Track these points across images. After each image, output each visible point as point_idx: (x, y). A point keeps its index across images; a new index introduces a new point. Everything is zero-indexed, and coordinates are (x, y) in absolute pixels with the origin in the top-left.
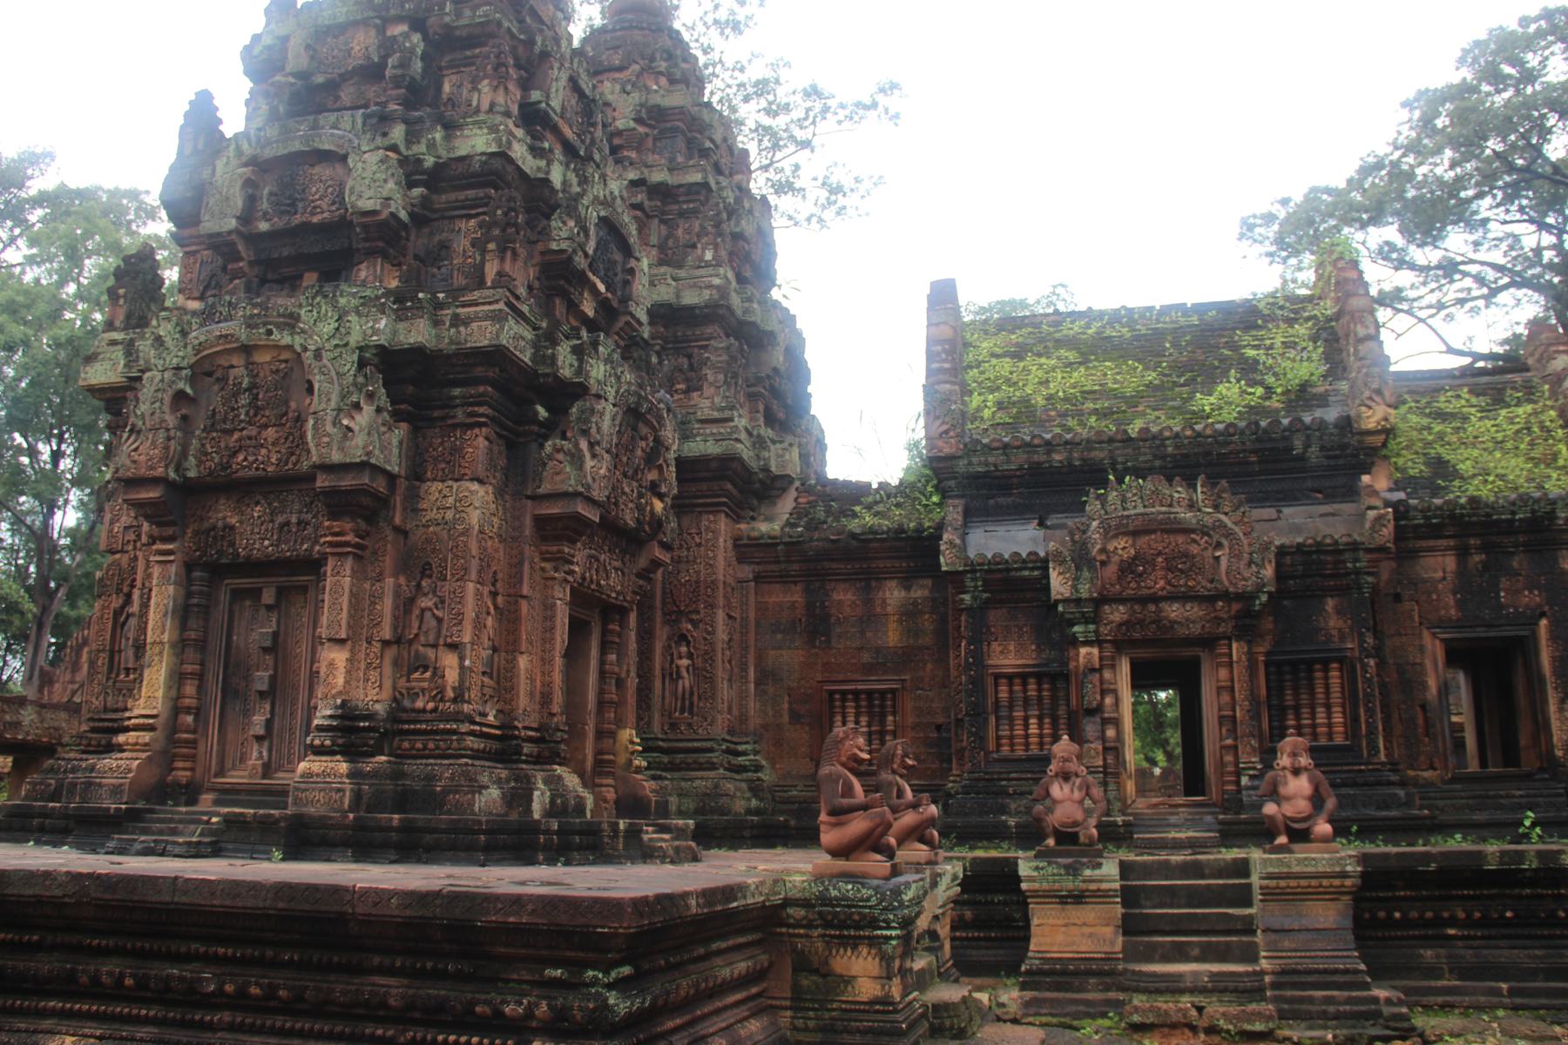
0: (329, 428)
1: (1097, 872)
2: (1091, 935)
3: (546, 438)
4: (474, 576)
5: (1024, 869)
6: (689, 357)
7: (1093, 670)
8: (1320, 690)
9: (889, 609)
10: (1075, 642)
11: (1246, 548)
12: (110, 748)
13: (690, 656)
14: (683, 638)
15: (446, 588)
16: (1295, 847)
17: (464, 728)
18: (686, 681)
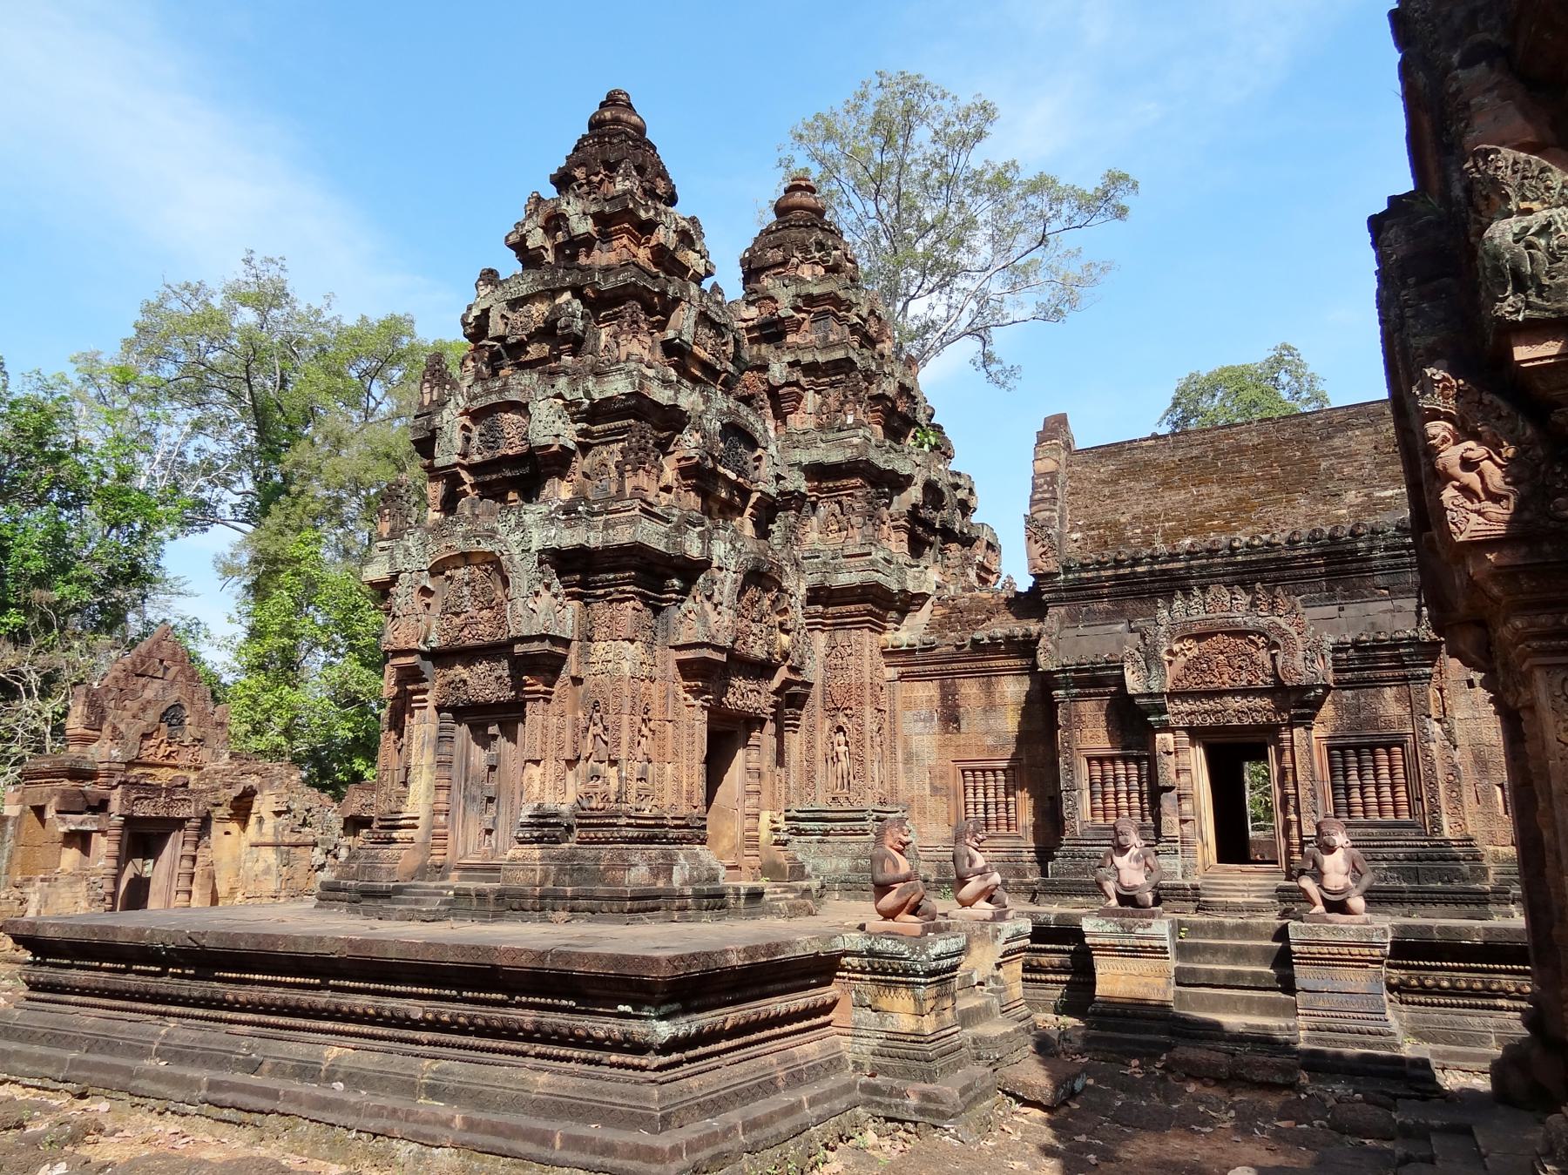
1: (1148, 931)
2: (1146, 985)
3: (682, 601)
4: (627, 710)
5: (1087, 925)
6: (840, 503)
7: (1169, 753)
8: (1384, 772)
9: (1008, 700)
10: (1151, 731)
11: (1301, 647)
12: (393, 841)
13: (847, 744)
14: (840, 729)
15: (610, 719)
16: (1331, 916)
17: (623, 821)
18: (844, 763)
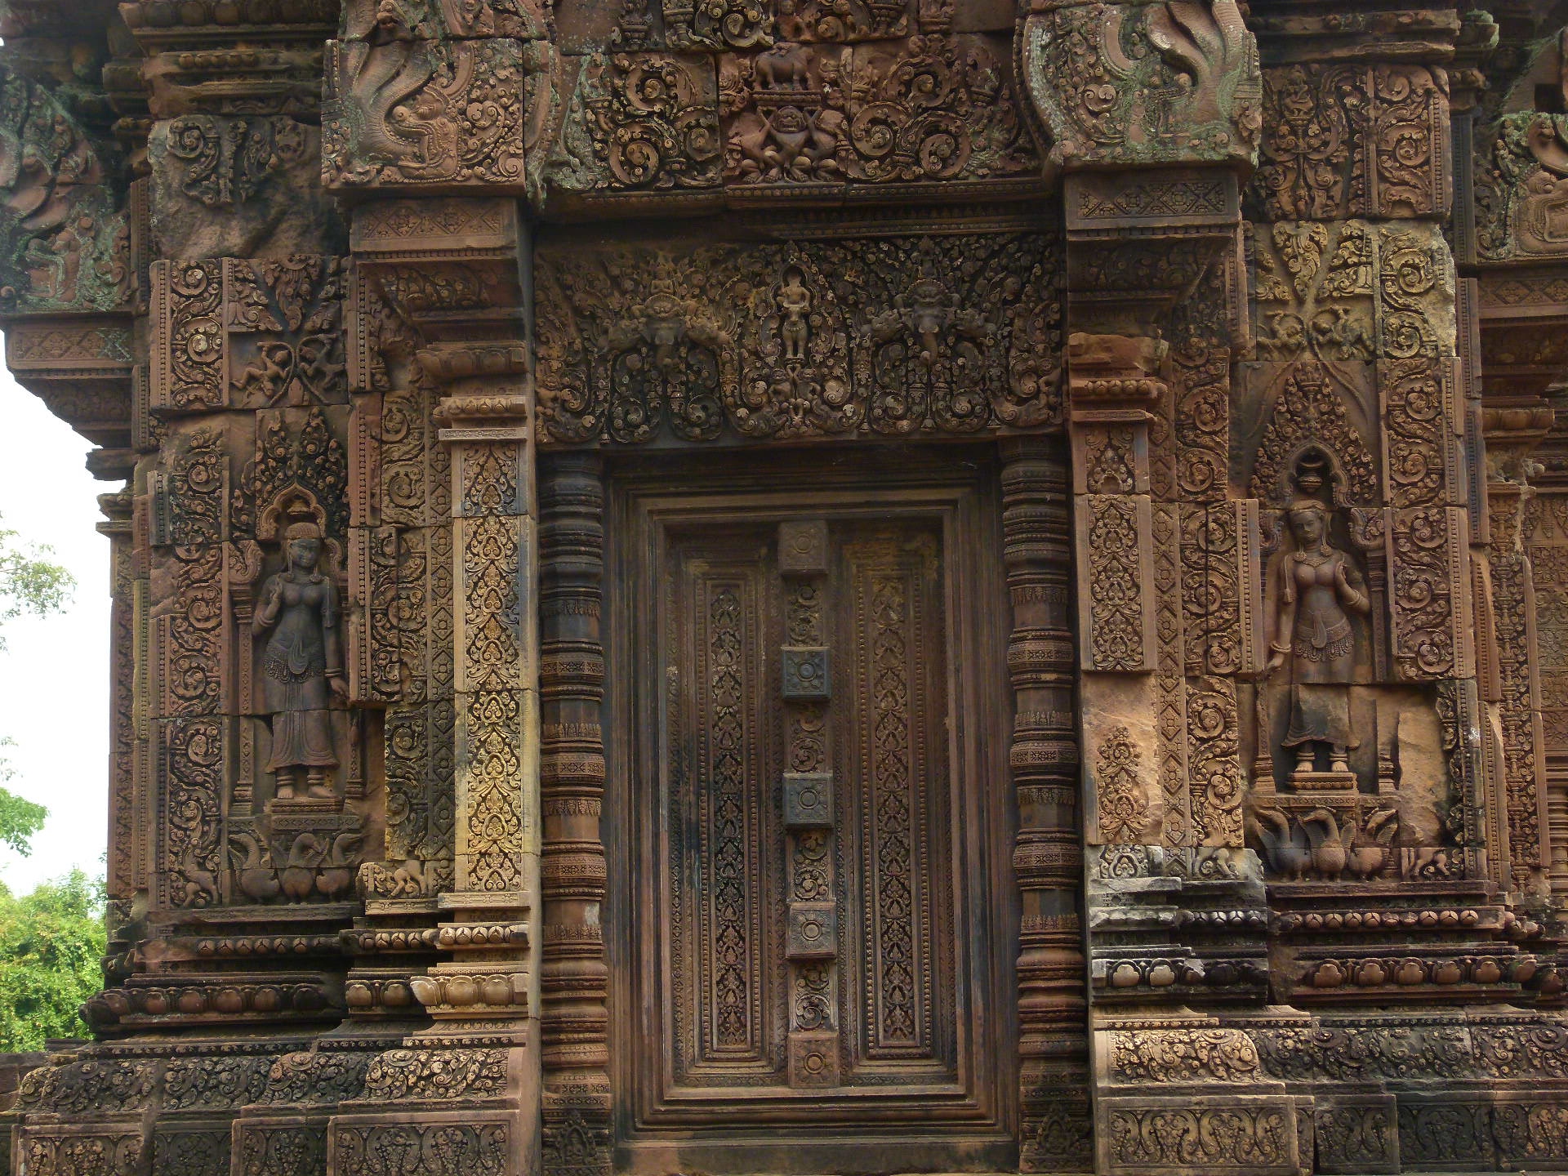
0: (1114, 57)
